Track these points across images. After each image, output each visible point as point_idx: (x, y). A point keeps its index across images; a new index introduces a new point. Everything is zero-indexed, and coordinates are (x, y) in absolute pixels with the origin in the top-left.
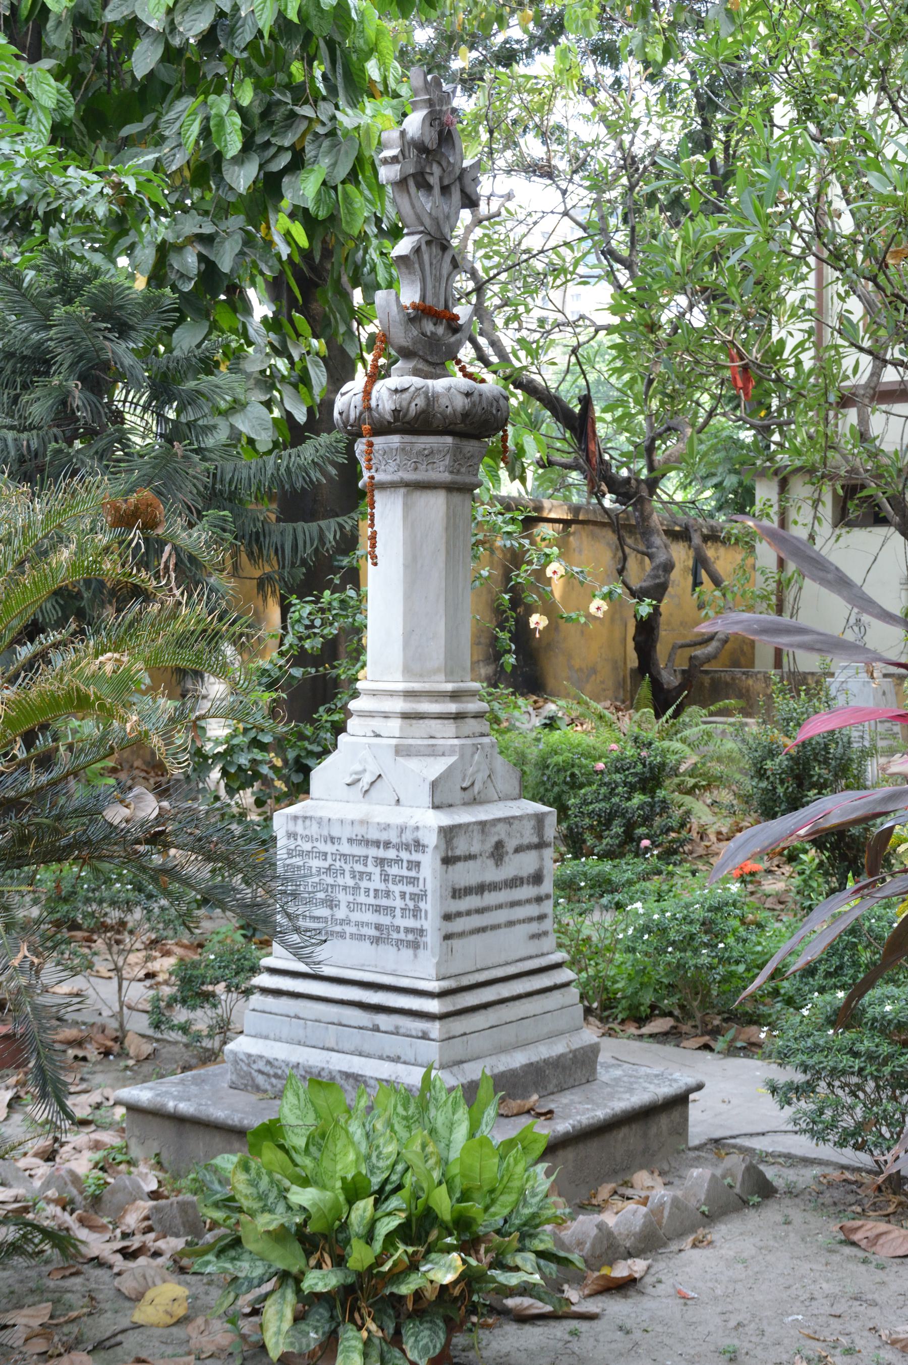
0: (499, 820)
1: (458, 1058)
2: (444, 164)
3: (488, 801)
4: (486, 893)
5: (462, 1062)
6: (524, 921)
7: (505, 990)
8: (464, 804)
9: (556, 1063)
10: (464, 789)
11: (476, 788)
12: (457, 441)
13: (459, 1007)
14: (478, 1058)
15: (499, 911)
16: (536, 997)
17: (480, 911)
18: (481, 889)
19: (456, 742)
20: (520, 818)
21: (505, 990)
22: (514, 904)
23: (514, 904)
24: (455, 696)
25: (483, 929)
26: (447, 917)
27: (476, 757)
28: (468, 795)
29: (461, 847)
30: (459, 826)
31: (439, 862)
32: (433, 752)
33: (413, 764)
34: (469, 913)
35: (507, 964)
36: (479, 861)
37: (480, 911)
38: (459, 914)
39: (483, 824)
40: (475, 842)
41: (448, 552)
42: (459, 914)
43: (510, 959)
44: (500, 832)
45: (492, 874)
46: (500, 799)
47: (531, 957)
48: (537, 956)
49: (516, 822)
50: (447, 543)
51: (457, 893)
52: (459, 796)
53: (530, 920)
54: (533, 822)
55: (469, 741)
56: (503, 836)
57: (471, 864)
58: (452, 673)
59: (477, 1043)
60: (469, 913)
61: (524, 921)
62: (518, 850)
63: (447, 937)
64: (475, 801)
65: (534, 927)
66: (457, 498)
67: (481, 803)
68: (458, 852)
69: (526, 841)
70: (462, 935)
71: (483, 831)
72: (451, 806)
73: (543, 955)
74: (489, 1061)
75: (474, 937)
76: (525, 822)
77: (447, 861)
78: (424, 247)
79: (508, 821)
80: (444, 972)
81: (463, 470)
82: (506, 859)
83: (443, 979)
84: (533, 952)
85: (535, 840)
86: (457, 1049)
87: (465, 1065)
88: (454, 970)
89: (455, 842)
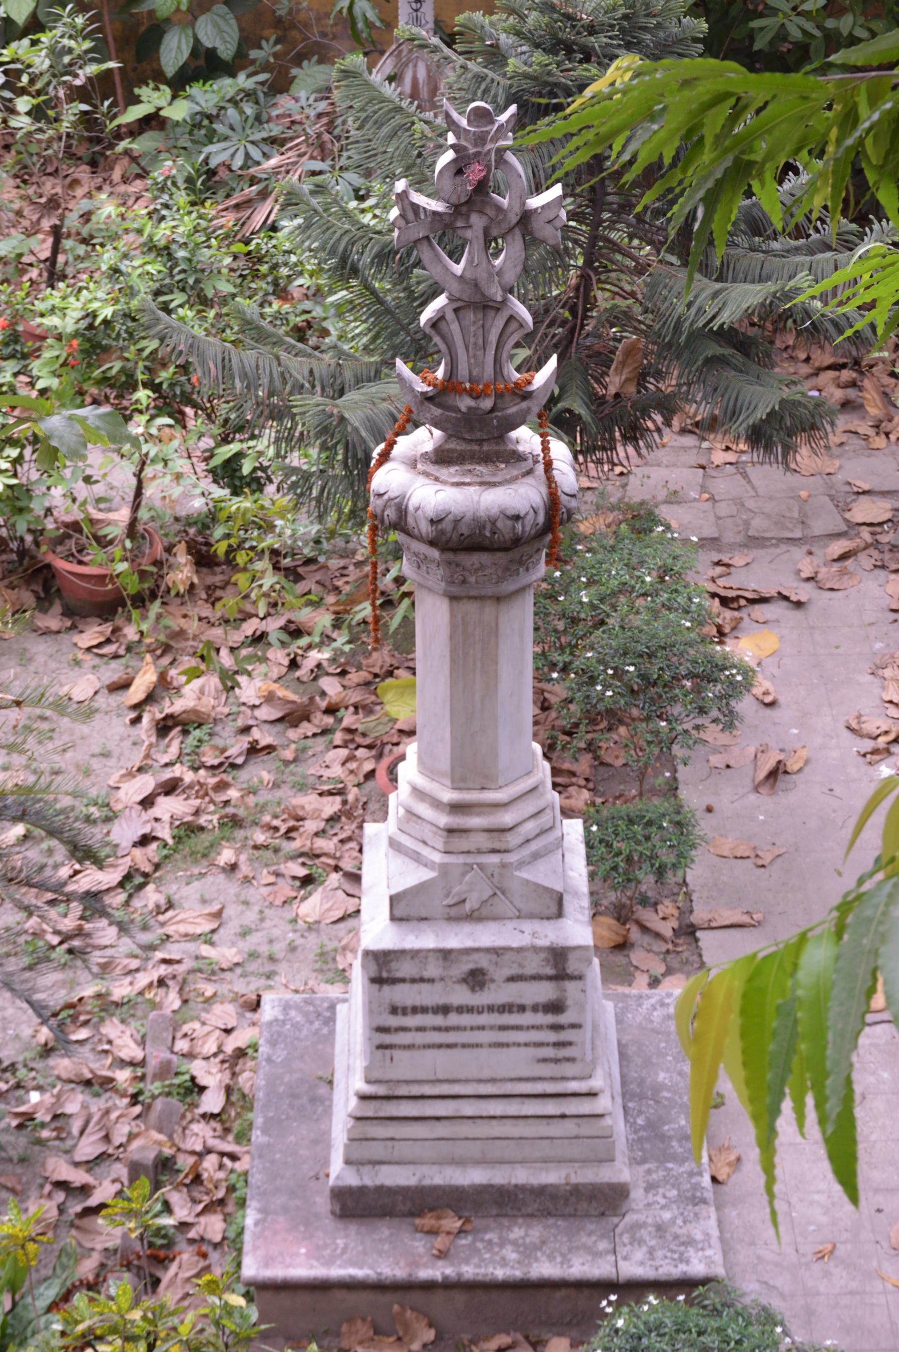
1: (377, 1157)
3: (495, 918)
6: (526, 1045)
7: (469, 1108)
8: (450, 919)
9: (541, 1191)
11: (468, 907)
12: (450, 556)
13: (382, 1114)
17: (438, 1029)
18: (445, 1010)
19: (437, 857)
20: (520, 950)
21: (469, 1108)
22: (503, 1028)
23: (503, 1028)
24: (456, 808)
25: (449, 1046)
26: (382, 1030)
27: (467, 878)
28: (453, 912)
29: (405, 969)
30: (403, 952)
31: (367, 982)
32: (417, 858)
33: (399, 862)
35: (493, 1080)
36: (438, 986)
37: (438, 1029)
39: (446, 954)
41: (453, 661)
43: (499, 1076)
44: (484, 962)
45: (461, 996)
46: (519, 917)
50: (453, 651)
54: (543, 955)
55: (461, 859)
57: (424, 986)
58: (464, 779)
59: (404, 1150)
61: (526, 1045)
62: (512, 979)
63: (380, 1047)
65: (550, 1052)
66: (471, 608)
67: (480, 919)
68: (399, 975)
69: (530, 970)
73: (564, 1079)
75: (430, 1053)
76: (528, 954)
77: (378, 981)
78: (450, 316)
80: (376, 1075)
81: (472, 579)
82: (493, 986)
85: (550, 971)
86: (376, 1150)
87: (384, 1168)
89: (393, 965)
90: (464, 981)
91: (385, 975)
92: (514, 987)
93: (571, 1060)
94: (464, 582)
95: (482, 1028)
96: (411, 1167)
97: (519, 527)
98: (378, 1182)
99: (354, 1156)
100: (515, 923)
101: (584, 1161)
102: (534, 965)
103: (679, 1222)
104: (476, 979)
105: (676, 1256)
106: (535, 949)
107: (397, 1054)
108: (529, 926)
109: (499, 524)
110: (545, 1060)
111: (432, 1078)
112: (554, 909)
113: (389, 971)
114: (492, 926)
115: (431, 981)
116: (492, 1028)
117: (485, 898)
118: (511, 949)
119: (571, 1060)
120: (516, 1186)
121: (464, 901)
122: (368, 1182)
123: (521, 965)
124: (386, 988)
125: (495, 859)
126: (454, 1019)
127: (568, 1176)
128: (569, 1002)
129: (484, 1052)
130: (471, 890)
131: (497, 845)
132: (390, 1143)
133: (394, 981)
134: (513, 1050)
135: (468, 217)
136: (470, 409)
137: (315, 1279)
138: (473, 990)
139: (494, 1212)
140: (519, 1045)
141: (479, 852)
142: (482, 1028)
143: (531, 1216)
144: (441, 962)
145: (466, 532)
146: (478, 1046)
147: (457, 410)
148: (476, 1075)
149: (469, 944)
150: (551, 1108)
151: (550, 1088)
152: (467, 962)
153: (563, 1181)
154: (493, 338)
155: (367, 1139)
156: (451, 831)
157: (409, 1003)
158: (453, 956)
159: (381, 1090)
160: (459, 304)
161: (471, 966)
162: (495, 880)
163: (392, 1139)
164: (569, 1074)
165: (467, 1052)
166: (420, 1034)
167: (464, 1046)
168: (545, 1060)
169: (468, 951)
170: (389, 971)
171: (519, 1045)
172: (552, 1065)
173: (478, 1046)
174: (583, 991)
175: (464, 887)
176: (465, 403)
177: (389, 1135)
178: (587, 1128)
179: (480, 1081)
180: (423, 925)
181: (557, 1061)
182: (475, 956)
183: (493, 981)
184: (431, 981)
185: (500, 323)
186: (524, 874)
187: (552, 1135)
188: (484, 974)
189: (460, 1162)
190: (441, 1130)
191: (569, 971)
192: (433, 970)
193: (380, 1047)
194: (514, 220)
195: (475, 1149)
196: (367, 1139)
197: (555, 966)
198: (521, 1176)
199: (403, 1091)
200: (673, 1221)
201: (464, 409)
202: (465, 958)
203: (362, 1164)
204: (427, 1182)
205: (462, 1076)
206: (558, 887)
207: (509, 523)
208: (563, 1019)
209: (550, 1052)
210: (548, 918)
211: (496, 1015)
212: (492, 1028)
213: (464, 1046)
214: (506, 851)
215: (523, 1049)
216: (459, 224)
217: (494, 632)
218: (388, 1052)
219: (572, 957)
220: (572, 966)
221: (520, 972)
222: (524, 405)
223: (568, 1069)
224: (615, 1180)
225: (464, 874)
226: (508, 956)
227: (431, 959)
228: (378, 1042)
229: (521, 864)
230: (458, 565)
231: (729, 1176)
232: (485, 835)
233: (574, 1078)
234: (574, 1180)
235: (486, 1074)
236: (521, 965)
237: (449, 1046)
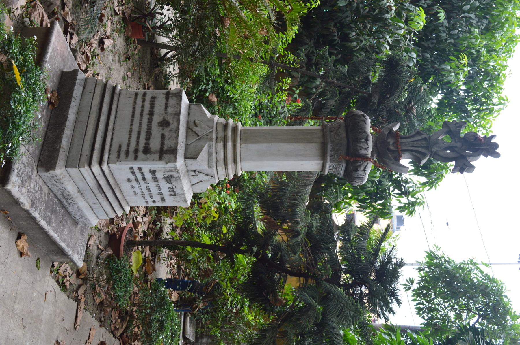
0: (179, 124)
1: (86, 88)
2: (463, 148)
4: (148, 116)
5: (84, 89)
6: (129, 141)
7: (103, 118)
8: (188, 123)
9: (59, 138)
10: (194, 122)
12: (344, 125)
13: (107, 90)
14: (81, 98)
15: (138, 124)
16: (92, 139)
17: (142, 112)
18: (151, 114)
20: (177, 138)
21: (103, 118)
22: (139, 133)
23: (139, 133)
24: (235, 129)
25: (133, 116)
28: (192, 124)
29: (172, 102)
34: (143, 106)
35: (113, 130)
36: (163, 112)
37: (142, 112)
38: (144, 101)
39: (178, 114)
40: (172, 109)
42: (144, 101)
43: (115, 132)
44: (173, 126)
45: (157, 119)
46: (187, 144)
47: (111, 146)
48: (110, 150)
49: (176, 135)
51: (153, 99)
52: (192, 119)
53: (128, 145)
54: (173, 146)
56: (172, 126)
57: (163, 107)
59: (88, 96)
60: (143, 106)
61: (129, 141)
62: (163, 136)
64: (189, 129)
65: (124, 148)
66: (320, 134)
68: (170, 100)
70: (135, 102)
71: (176, 114)
72: (189, 114)
73: (109, 154)
74: (78, 100)
76: (175, 141)
79: (177, 130)
81: (332, 134)
82: (160, 129)
83: (120, 93)
84: (113, 148)
85: (165, 148)
86: (90, 86)
87: (82, 89)
88: (122, 96)
90: (164, 120)
91: (170, 95)
92: (159, 136)
93: (119, 156)
94: (331, 131)
95: (140, 125)
96: (80, 97)
97: (363, 140)
98: (76, 84)
99: (89, 81)
100: (184, 142)
101: (68, 157)
102: (168, 143)
103: (29, 188)
104: (164, 124)
105: (20, 173)
106: (176, 144)
107: (132, 99)
108: (183, 145)
109: (364, 134)
110: (120, 147)
111: (118, 110)
112: (189, 156)
113: (172, 97)
114: (185, 134)
115: (166, 109)
116: (140, 129)
117: (197, 133)
118: (178, 135)
119: (119, 156)
120: (64, 129)
121: (196, 126)
122: (77, 81)
123: (169, 139)
124: (164, 96)
125: (214, 137)
126: (146, 117)
127: (64, 149)
128: (148, 155)
129: (129, 127)
130: (201, 128)
131: (219, 139)
132: (93, 91)
133: (167, 98)
134: (128, 136)
135: (460, 142)
136: (389, 142)
137: (50, 42)
138: (159, 123)
139: (51, 122)
140: (130, 138)
141: (217, 133)
142: (140, 125)
143: (46, 134)
144: (174, 112)
145: (361, 123)
146: (132, 124)
147: (387, 139)
148: (117, 123)
149: (181, 123)
150: (98, 146)
151: (107, 147)
152: (173, 121)
153: (62, 146)
154: (417, 149)
155: (96, 85)
156: (226, 126)
157: (156, 103)
158: (176, 116)
159: (117, 92)
160: (428, 139)
161: (171, 122)
162: (205, 137)
163: (94, 93)
164: (111, 156)
165: (130, 121)
166: (141, 106)
167: (132, 121)
168: (120, 147)
169: (178, 121)
170: (172, 97)
171: (130, 138)
172: (117, 150)
173: (132, 124)
174: (153, 160)
175: (203, 126)
176: (391, 141)
177: (96, 92)
178: (85, 158)
179: (114, 125)
180: (187, 113)
181: (119, 152)
182: (176, 124)
183: (163, 129)
184: (166, 109)
185: (423, 150)
186: (206, 147)
187: (84, 146)
188: (166, 127)
189: (78, 113)
190: (95, 109)
191: (164, 155)
192: (170, 110)
193: (136, 94)
194: (463, 154)
195: (83, 117)
196: (96, 85)
197: (167, 150)
198: (67, 132)
199: (116, 98)
200: (30, 186)
201: (388, 141)
202: (175, 120)
203: (85, 82)
204: (73, 100)
205: (117, 119)
206: (199, 158)
207: (365, 137)
208: (140, 154)
209: (124, 148)
210: (185, 154)
211: (146, 130)
212: (140, 129)
213: (132, 121)
214: (216, 142)
215: (128, 139)
216: (456, 140)
217: (309, 141)
218: (134, 96)
219: (172, 156)
220: (166, 157)
221: (166, 138)
222: (392, 159)
223: (114, 156)
224: (57, 165)
225: (209, 126)
226: (174, 135)
227: (176, 109)
228: (139, 93)
229: (210, 147)
230: (339, 128)
231: (17, 246)
232: (223, 136)
233: (109, 158)
234: (61, 150)
235: (117, 127)
236: (169, 139)
237: (133, 116)
